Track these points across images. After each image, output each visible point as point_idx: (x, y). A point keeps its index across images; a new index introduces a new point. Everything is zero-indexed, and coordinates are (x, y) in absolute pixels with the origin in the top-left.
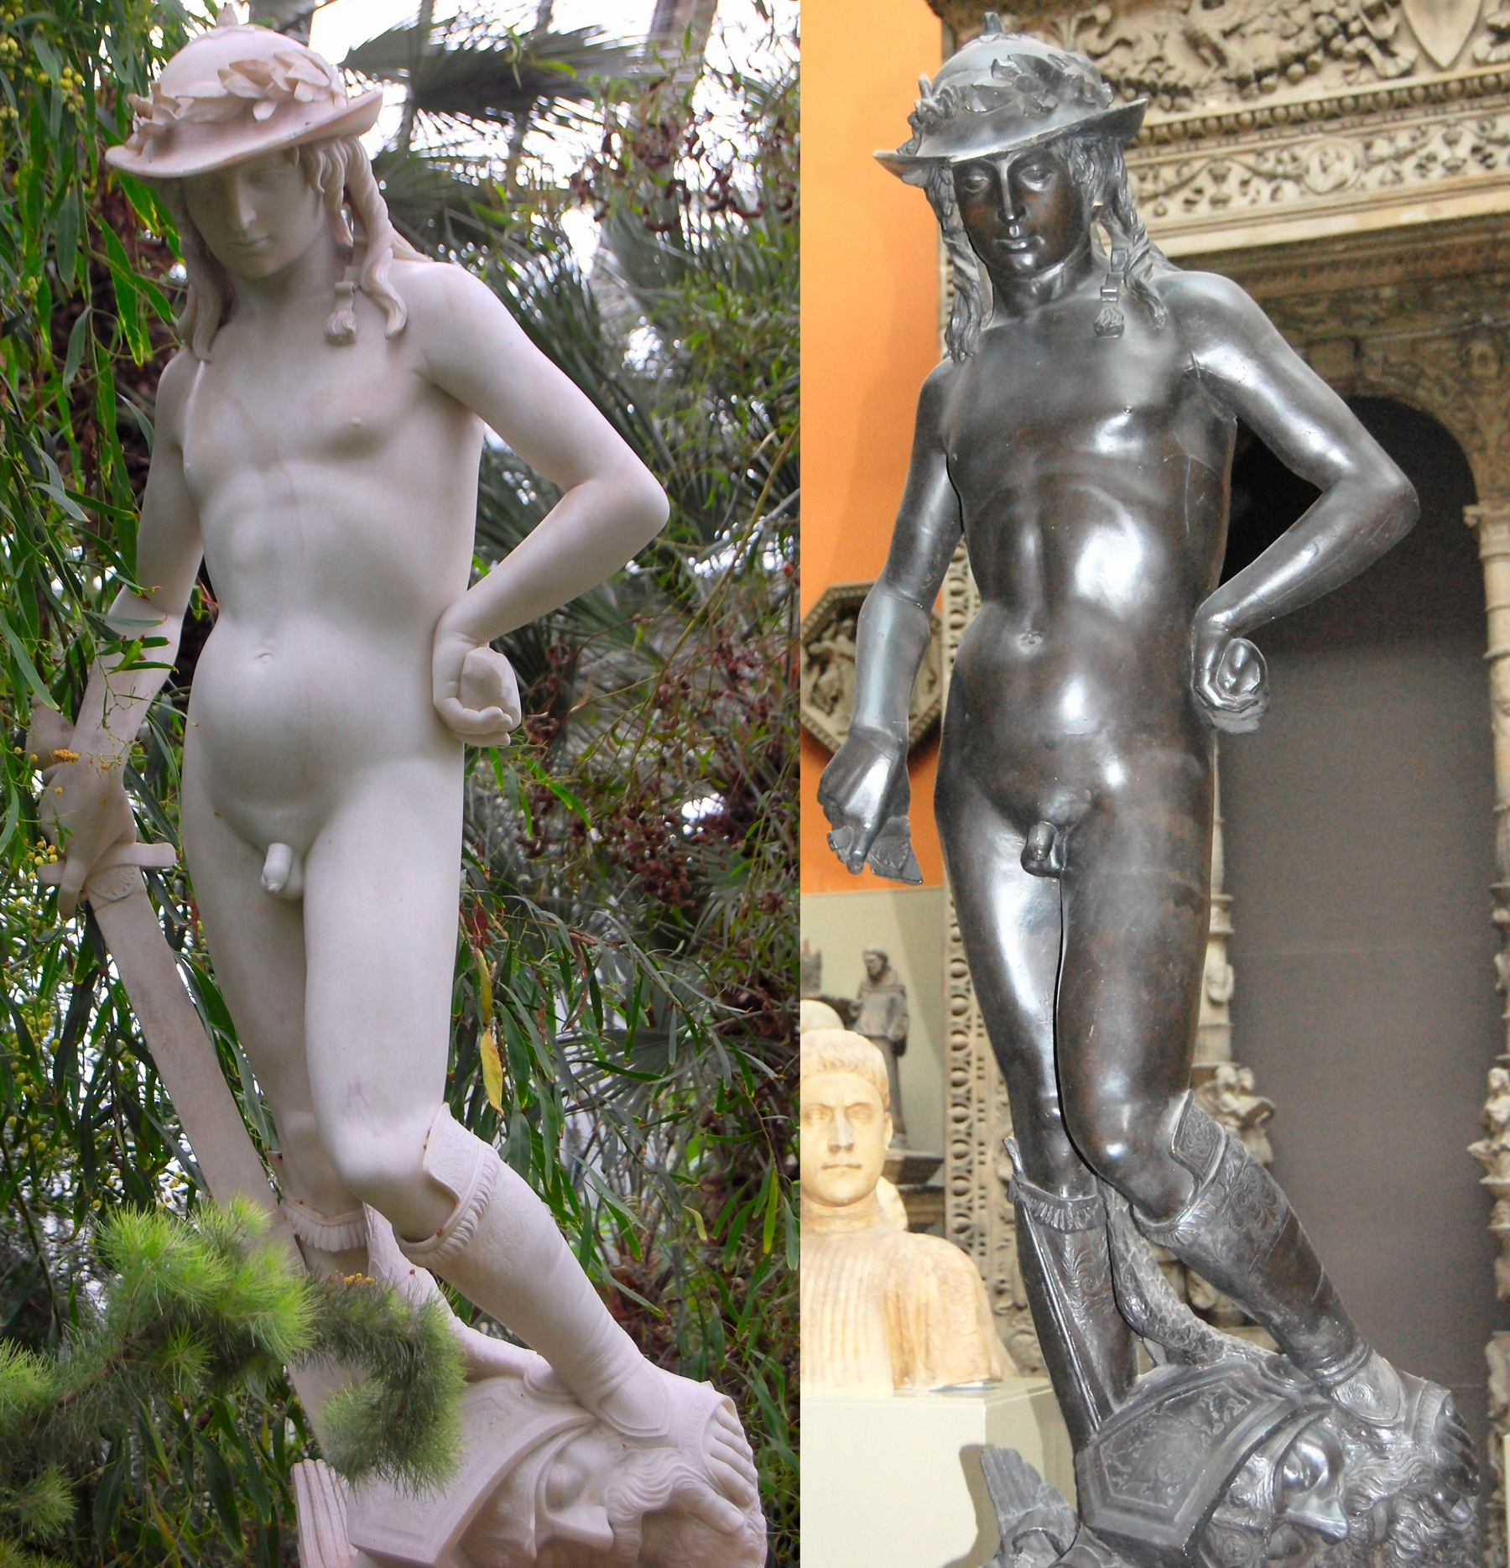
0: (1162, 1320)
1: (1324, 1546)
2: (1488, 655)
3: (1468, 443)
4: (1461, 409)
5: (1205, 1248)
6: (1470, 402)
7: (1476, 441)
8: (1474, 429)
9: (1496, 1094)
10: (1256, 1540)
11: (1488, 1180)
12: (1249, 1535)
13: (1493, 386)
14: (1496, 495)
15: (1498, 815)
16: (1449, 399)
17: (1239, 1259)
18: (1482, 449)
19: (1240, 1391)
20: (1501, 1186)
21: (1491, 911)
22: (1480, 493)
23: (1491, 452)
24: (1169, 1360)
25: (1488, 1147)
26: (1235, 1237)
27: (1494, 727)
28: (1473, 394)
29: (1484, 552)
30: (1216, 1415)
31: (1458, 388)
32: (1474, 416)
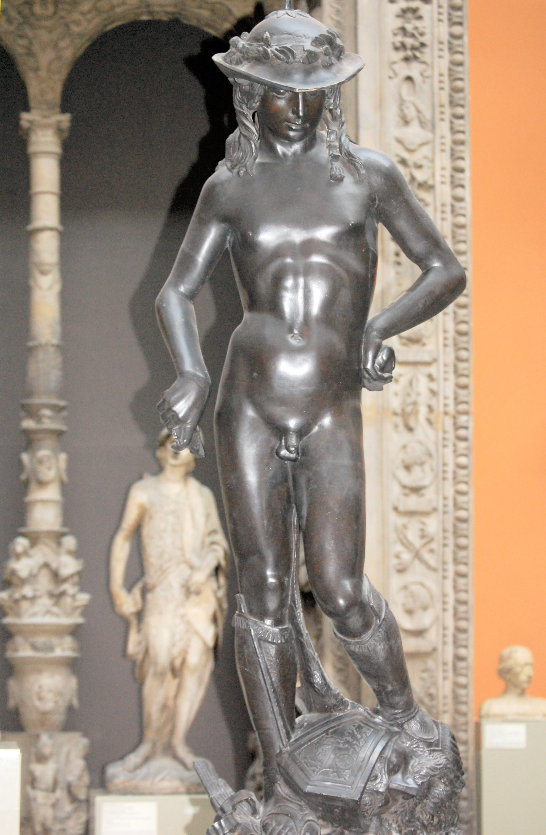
0: (331, 689)
1: (401, 800)
2: (30, 227)
3: (24, 65)
4: (21, 37)
5: (376, 652)
6: (29, 32)
7: (31, 62)
8: (30, 53)
9: (18, 557)
10: (379, 797)
11: (8, 620)
12: (375, 794)
13: (48, 23)
14: (44, 107)
15: (31, 350)
16: (12, 28)
17: (387, 659)
18: (37, 69)
19: (365, 724)
20: (14, 625)
21: (20, 420)
22: (32, 104)
23: (43, 73)
24: (310, 710)
25: (10, 596)
26: (387, 647)
27: (32, 283)
28: (31, 26)
29: (32, 149)
30: (359, 736)
31: (21, 20)
32: (31, 43)
